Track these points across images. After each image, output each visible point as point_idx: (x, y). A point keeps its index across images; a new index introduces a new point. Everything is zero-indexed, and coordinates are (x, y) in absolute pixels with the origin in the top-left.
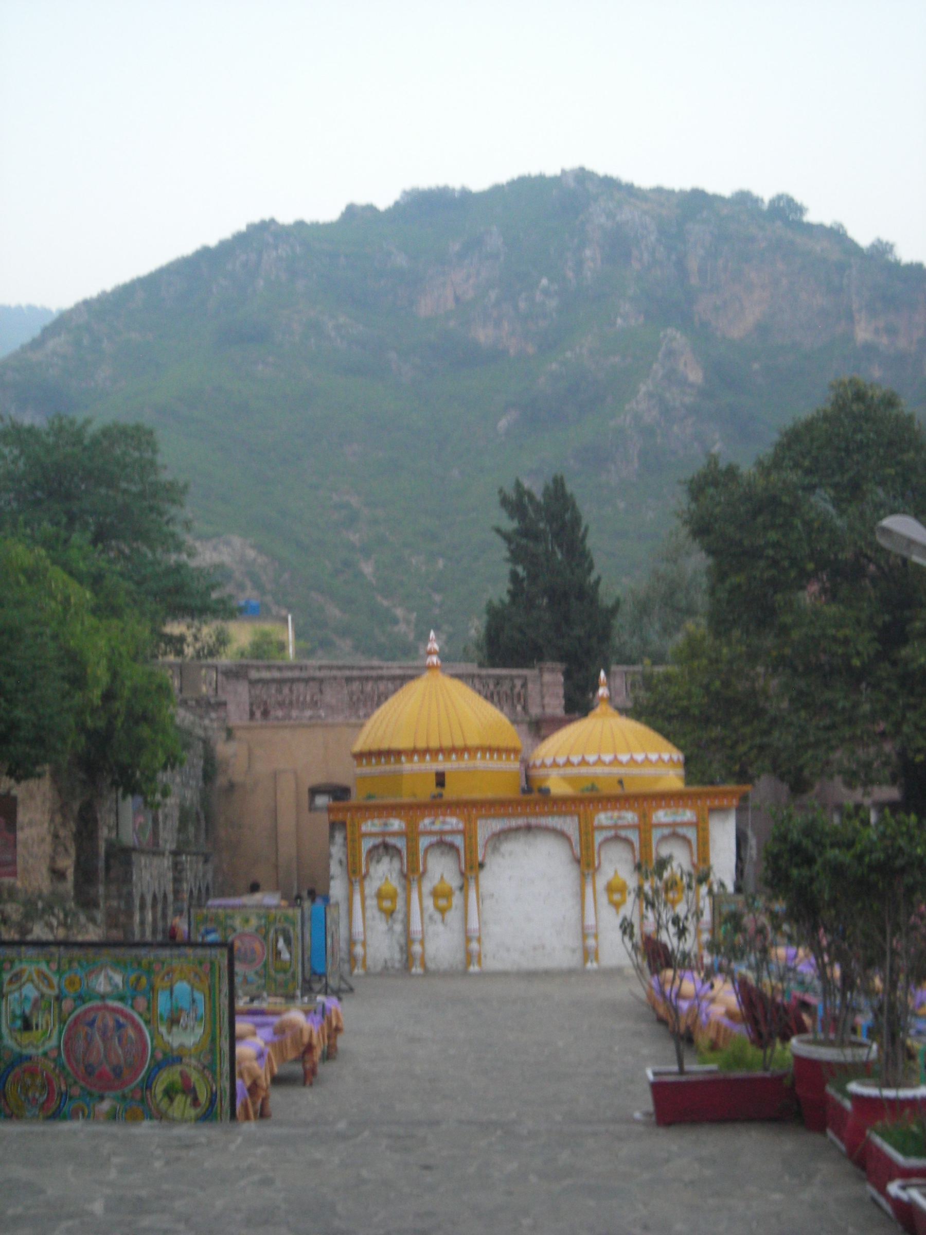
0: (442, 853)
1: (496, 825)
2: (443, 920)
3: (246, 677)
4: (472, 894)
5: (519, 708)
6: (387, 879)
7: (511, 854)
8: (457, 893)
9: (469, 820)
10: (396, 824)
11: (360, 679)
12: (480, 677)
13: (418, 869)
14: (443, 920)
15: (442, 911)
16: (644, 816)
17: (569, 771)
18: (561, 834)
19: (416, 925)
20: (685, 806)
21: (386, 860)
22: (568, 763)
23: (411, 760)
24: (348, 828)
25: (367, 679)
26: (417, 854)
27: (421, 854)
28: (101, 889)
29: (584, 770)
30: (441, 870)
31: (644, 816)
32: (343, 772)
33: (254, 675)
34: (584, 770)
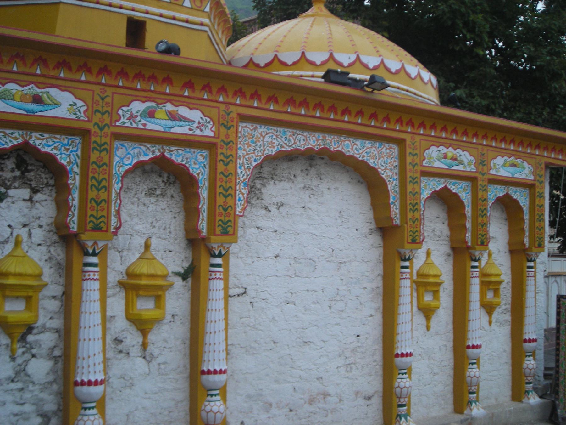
0: (151, 193)
1: (273, 141)
2: (144, 346)
6: (18, 243)
7: (280, 205)
8: (178, 282)
9: (223, 123)
10: (64, 104)
13: (108, 224)
14: (144, 346)
15: (143, 326)
16: (482, 162)
18: (367, 178)
19: (90, 366)
20: (525, 157)
21: (20, 193)
26: (108, 189)
27: (117, 186)
30: (146, 228)
31: (482, 162)
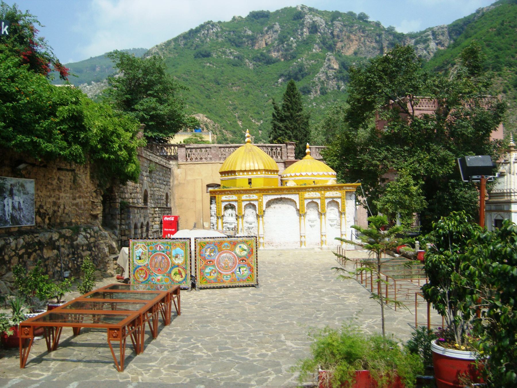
3: (185, 147)
4: (261, 222)
5: (279, 157)
11: (224, 147)
12: (265, 146)
17: (297, 178)
22: (296, 176)
23: (240, 175)
24: (217, 199)
25: (227, 147)
26: (242, 208)
28: (118, 222)
29: (301, 178)
32: (217, 179)
33: (187, 146)
34: (301, 178)
